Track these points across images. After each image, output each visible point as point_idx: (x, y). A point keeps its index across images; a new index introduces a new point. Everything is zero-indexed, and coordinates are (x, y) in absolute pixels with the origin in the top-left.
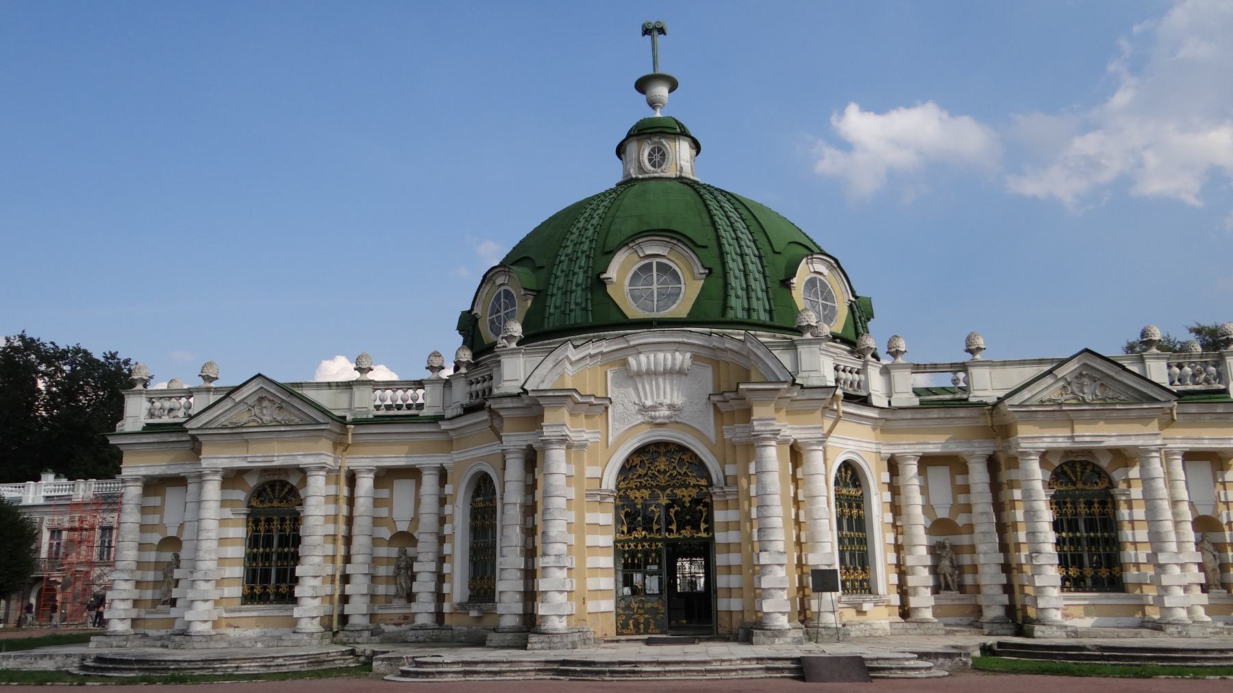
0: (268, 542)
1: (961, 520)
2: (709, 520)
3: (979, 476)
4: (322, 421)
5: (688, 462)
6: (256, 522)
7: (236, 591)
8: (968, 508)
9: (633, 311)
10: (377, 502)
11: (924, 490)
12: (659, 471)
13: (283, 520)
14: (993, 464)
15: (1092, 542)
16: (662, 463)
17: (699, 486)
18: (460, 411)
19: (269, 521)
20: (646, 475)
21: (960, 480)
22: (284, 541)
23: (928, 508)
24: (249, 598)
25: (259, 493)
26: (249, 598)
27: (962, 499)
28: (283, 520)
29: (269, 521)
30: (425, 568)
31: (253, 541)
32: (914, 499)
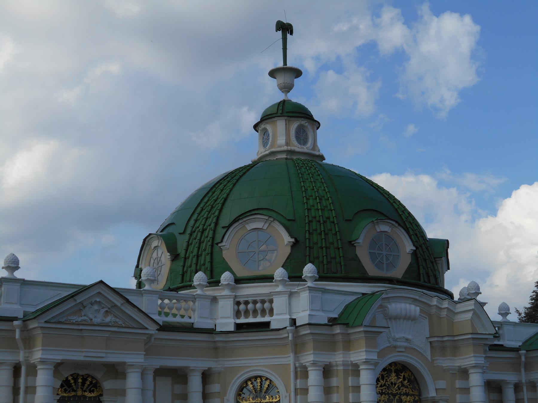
4: (135, 327)
5: (407, 378)
9: (371, 270)
12: (392, 383)
16: (393, 378)
17: (413, 395)
18: (232, 328)
20: (385, 385)
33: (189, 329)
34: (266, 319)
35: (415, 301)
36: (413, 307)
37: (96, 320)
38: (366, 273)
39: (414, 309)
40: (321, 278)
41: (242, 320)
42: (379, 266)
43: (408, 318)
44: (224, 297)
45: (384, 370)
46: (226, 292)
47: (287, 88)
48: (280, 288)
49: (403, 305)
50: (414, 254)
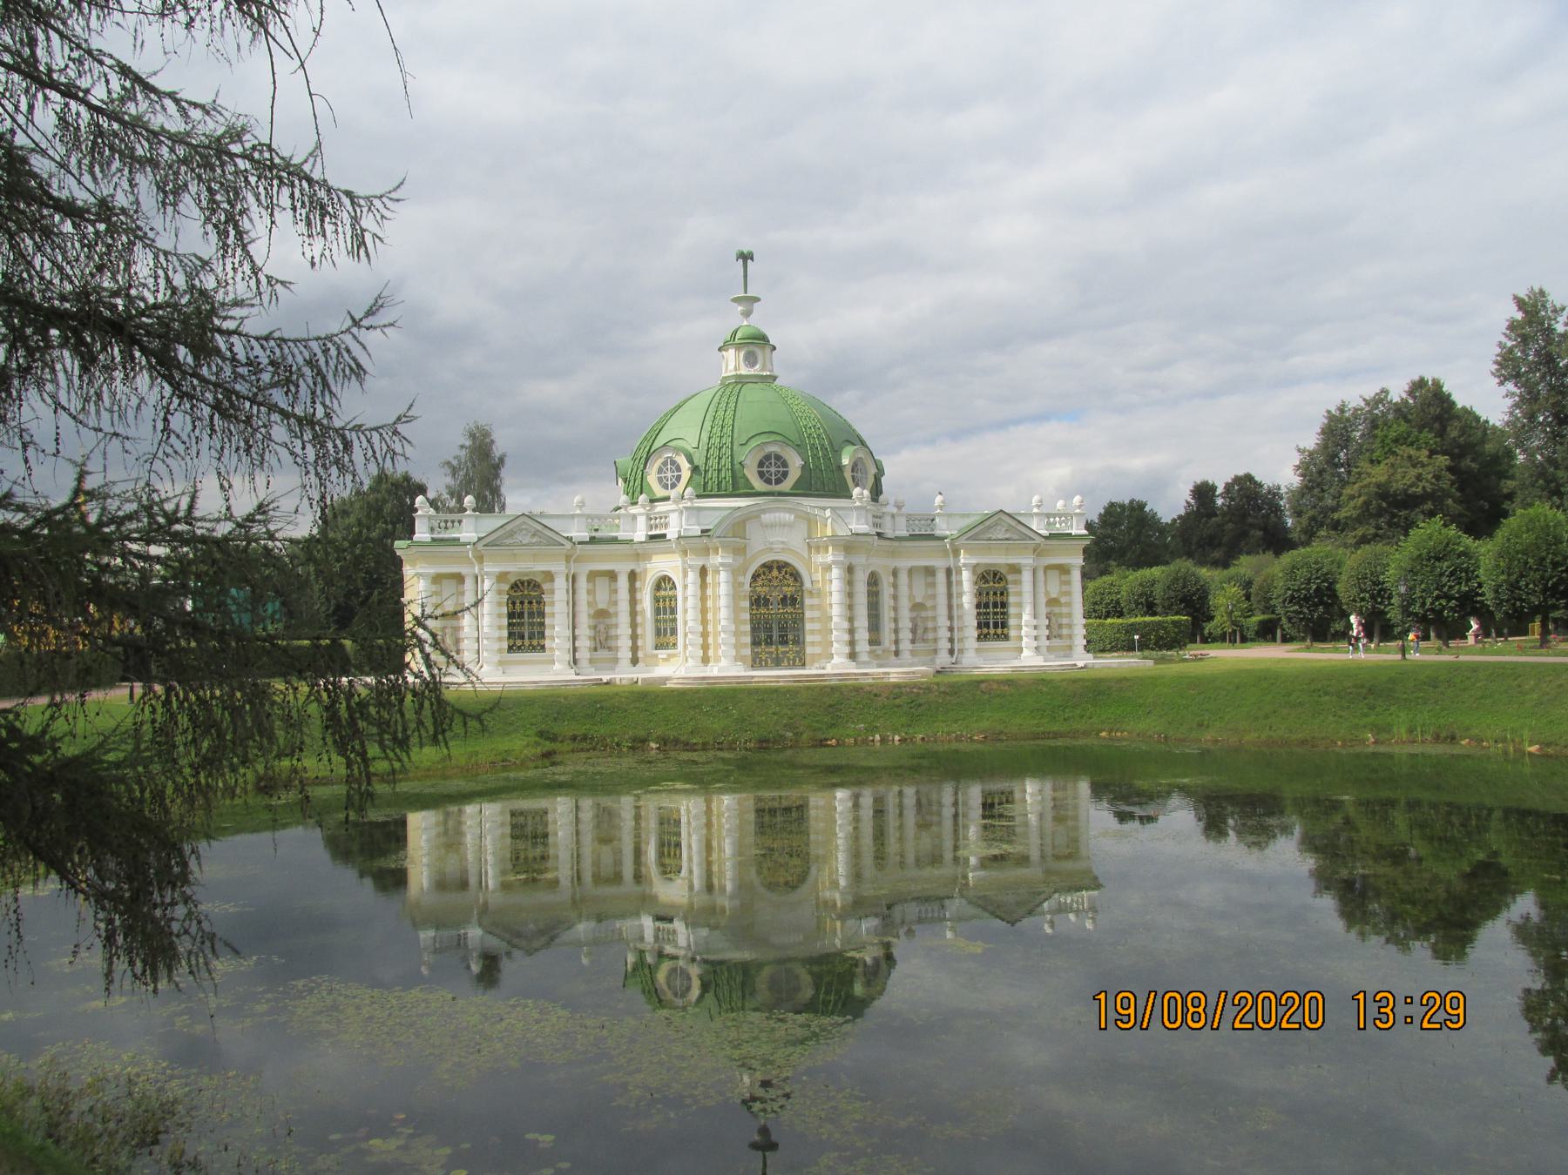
0: (521, 615)
1: (929, 604)
2: (802, 603)
3: (941, 577)
6: (514, 603)
7: (506, 646)
8: (934, 597)
10: (589, 592)
11: (910, 587)
13: (530, 603)
14: (949, 572)
15: (995, 614)
19: (522, 603)
21: (930, 579)
22: (531, 615)
23: (911, 597)
24: (510, 649)
25: (515, 586)
26: (510, 649)
27: (930, 592)
28: (530, 603)
29: (522, 603)
30: (624, 630)
31: (511, 615)
32: (904, 590)
33: (614, 540)
34: (663, 532)
35: (790, 511)
36: (787, 516)
37: (525, 542)
38: (753, 488)
39: (788, 517)
40: (699, 497)
41: (653, 532)
42: (768, 481)
43: (783, 525)
44: (641, 514)
45: (764, 566)
46: (642, 511)
47: (747, 314)
48: (674, 507)
49: (782, 515)
50: (803, 468)
